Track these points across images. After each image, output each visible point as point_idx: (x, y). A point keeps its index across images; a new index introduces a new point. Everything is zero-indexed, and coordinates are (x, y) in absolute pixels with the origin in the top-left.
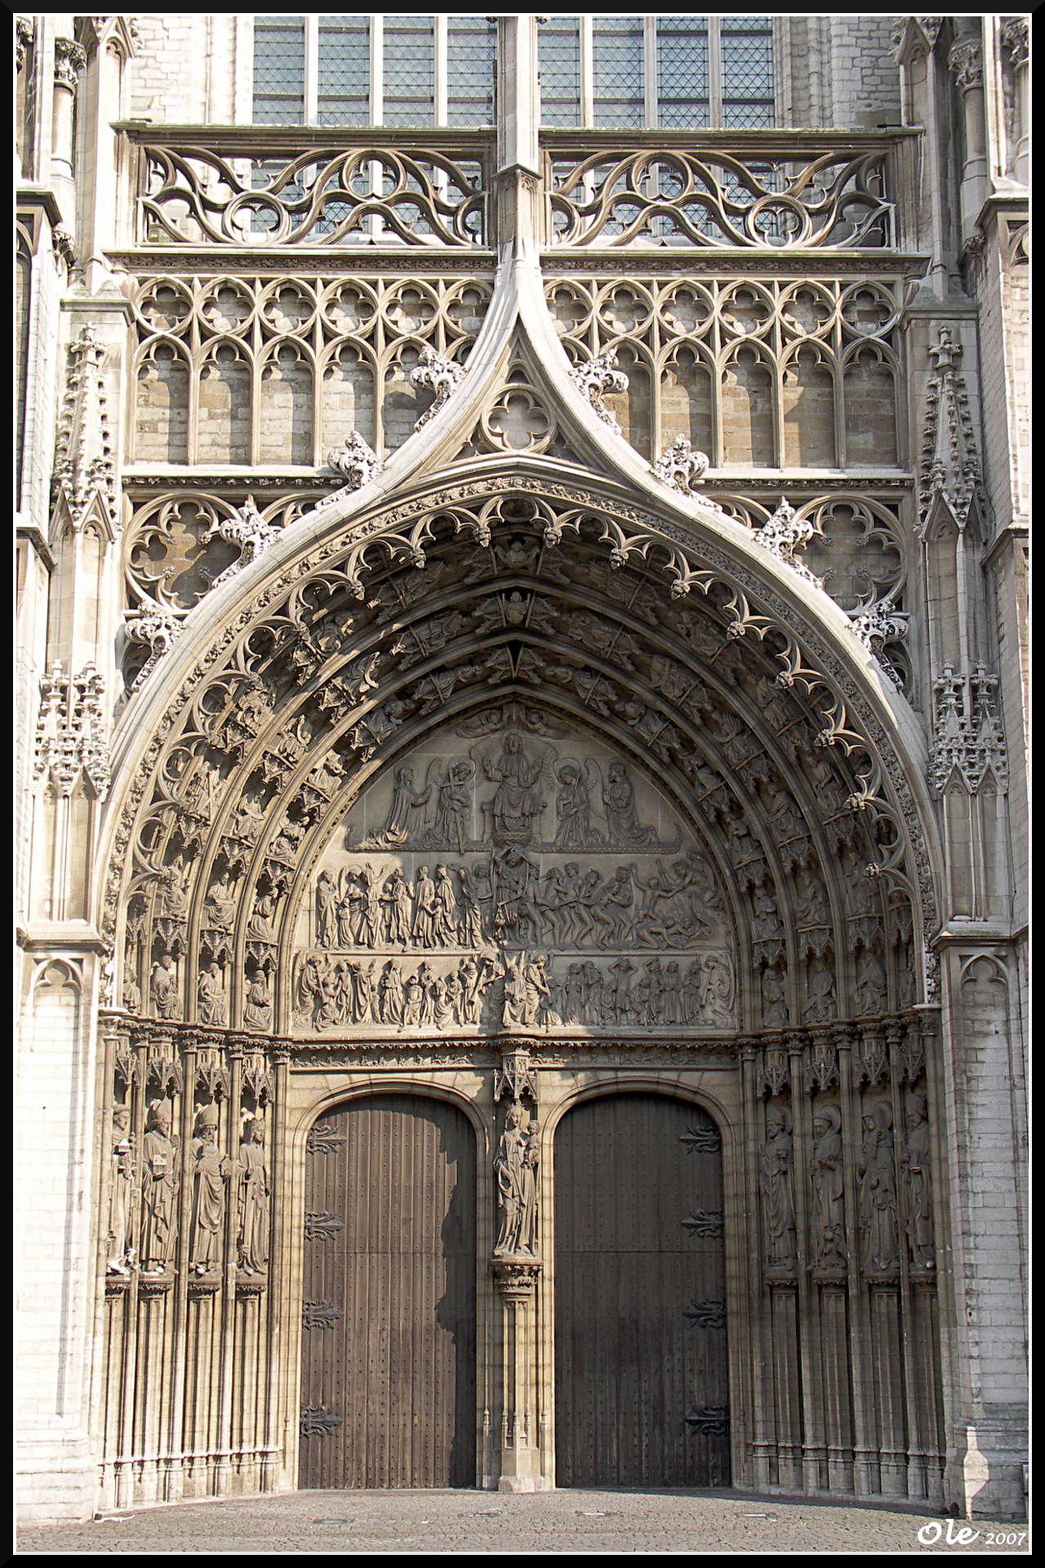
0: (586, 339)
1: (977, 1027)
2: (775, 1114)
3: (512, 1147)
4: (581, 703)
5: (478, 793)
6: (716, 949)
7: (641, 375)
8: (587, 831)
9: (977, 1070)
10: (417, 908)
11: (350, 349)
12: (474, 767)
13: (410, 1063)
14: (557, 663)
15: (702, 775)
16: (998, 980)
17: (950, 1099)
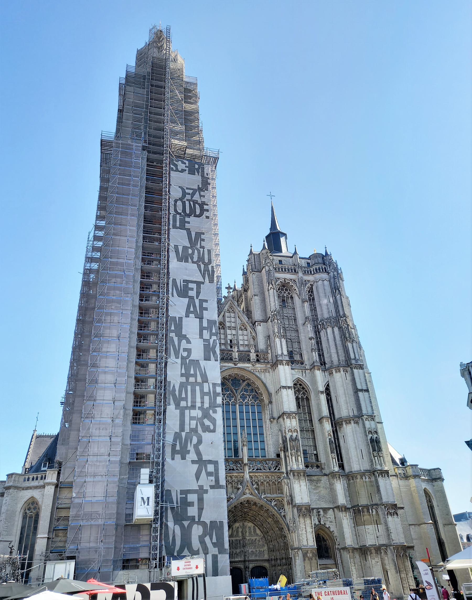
0: (253, 481)
1: (296, 559)
2: (273, 568)
3: (247, 573)
4: (251, 520)
5: (240, 530)
6: (266, 548)
7: (258, 485)
8: (252, 535)
9: (296, 564)
10: (235, 544)
11: (230, 482)
12: (240, 527)
13: (236, 564)
14: (249, 515)
15: (264, 528)
16: (298, 553)
17: (294, 567)
